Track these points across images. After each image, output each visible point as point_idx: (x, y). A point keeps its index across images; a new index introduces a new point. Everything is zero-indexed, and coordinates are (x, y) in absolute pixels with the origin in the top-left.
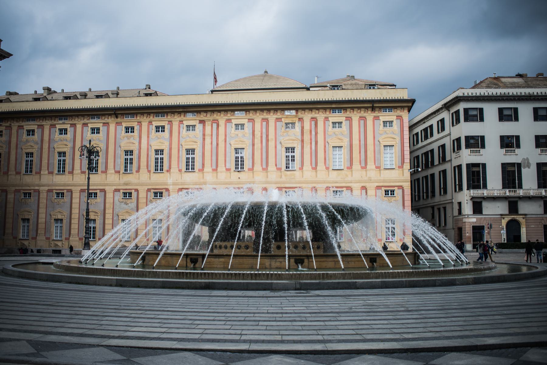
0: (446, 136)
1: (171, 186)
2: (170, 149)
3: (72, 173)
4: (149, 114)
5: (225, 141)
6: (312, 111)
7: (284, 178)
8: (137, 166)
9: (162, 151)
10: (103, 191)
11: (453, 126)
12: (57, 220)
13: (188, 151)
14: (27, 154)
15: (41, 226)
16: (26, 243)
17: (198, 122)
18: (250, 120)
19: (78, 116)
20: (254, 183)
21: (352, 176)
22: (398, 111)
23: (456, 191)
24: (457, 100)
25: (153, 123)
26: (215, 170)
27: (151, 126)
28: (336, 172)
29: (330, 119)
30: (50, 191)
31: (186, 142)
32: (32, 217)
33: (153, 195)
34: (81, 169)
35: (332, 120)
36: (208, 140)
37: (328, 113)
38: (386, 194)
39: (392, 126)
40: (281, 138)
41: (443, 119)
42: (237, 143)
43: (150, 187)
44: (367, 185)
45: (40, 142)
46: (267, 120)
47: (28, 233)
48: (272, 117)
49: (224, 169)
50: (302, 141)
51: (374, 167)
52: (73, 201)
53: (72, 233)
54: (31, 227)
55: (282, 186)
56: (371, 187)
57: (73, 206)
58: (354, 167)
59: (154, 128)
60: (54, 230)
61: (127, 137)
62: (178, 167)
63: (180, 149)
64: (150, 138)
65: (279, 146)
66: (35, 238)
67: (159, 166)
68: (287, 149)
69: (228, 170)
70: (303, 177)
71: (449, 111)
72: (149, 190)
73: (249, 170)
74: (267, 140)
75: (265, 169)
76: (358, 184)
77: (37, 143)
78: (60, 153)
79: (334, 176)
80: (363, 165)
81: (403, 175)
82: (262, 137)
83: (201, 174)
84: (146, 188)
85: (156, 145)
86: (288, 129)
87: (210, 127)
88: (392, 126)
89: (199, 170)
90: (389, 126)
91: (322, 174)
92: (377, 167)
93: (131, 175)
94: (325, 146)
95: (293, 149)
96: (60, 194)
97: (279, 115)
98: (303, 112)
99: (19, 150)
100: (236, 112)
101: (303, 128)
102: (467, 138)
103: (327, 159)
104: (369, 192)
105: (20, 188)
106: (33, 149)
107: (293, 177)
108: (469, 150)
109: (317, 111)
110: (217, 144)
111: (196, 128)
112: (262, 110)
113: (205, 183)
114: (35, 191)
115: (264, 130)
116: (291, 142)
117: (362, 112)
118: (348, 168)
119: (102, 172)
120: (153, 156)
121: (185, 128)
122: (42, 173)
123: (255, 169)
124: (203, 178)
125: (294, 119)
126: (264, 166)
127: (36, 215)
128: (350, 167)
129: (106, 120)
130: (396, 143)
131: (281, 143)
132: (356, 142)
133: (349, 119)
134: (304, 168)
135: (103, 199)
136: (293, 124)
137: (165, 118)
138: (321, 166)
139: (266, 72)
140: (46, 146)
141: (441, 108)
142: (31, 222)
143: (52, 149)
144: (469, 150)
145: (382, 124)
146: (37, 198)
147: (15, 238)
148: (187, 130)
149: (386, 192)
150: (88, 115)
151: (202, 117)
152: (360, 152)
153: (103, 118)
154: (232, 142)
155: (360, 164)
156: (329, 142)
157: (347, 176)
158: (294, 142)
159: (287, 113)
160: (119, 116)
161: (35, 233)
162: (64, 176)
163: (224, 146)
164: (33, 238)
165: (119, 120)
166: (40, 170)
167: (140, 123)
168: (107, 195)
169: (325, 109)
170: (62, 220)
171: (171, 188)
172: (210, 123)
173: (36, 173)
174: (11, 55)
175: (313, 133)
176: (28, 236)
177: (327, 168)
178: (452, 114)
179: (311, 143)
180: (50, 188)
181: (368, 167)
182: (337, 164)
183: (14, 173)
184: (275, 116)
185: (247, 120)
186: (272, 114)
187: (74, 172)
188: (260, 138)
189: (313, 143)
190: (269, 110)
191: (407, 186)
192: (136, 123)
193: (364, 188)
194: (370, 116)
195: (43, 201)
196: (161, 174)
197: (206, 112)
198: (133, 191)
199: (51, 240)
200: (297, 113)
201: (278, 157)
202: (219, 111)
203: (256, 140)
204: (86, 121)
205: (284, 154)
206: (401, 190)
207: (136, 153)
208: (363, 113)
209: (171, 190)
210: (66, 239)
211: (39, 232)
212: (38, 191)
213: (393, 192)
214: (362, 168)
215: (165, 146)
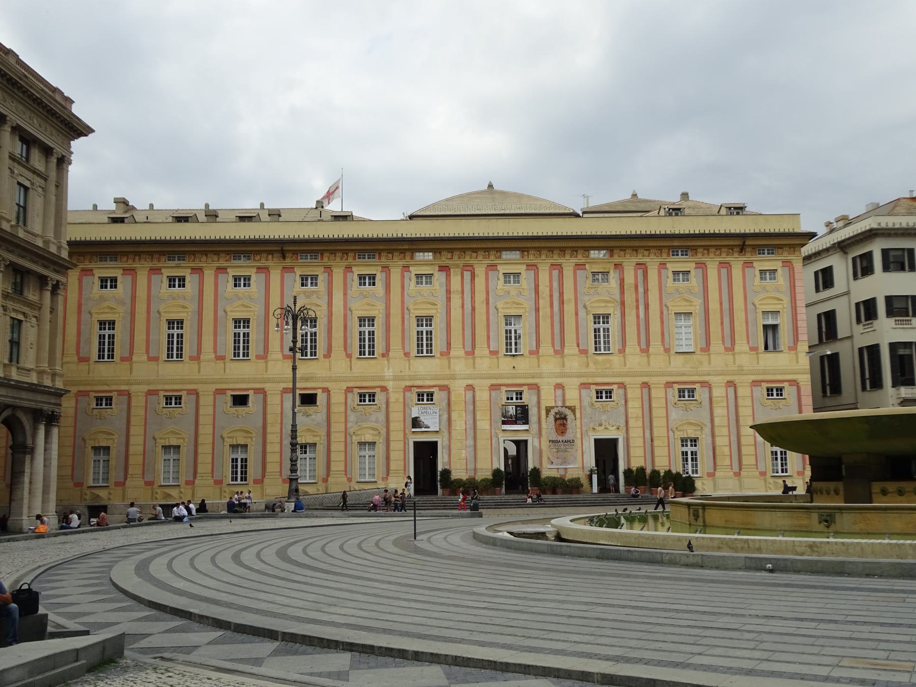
0: (837, 297)
1: (391, 383)
2: (388, 316)
3: (196, 358)
4: (346, 252)
5: (488, 303)
6: (636, 251)
7: (592, 368)
8: (326, 346)
9: (372, 320)
10: (262, 392)
11: (855, 277)
12: (166, 448)
13: (420, 320)
14: (102, 323)
15: (135, 461)
16: (103, 493)
17: (437, 268)
18: (531, 266)
19: (206, 253)
20: (540, 376)
21: (710, 363)
22: (785, 254)
23: (864, 388)
24: (871, 235)
25: (354, 269)
26: (471, 353)
27: (349, 275)
28: (682, 357)
29: (668, 265)
30: (151, 393)
31: (415, 304)
32: (115, 444)
33: (357, 398)
34: (215, 351)
35: (672, 267)
36: (456, 301)
37: (664, 255)
38: (768, 395)
39: (775, 279)
40: (586, 298)
41: (831, 268)
42: (509, 306)
43: (351, 384)
44: (736, 379)
45: (128, 301)
46: (559, 267)
47: (107, 473)
48: (568, 263)
49: (488, 352)
50: (623, 303)
51: (747, 348)
52: (201, 412)
53: (199, 471)
54: (113, 463)
55: (590, 380)
56: (744, 382)
57: (202, 420)
58: (712, 348)
59: (356, 278)
60: (161, 466)
61: (305, 293)
62: (403, 348)
63: (406, 317)
64: (349, 296)
65: (582, 313)
66: (121, 484)
67: (367, 348)
68: (596, 317)
69: (494, 353)
70: (625, 365)
71: (846, 253)
72: (349, 390)
73: (531, 353)
74: (562, 302)
75: (560, 352)
76: (721, 377)
77: (122, 303)
78: (171, 323)
79: (678, 363)
81: (797, 362)
82: (551, 296)
83: (445, 361)
84: (344, 385)
85: (359, 309)
86: (596, 283)
87: (459, 278)
88: (775, 279)
89: (442, 354)
91: (658, 360)
92: (752, 349)
93: (314, 362)
94: (662, 313)
95: (606, 318)
96: (174, 400)
97: (580, 259)
98: (622, 253)
99: (85, 316)
100: (504, 253)
101: (622, 281)
102: (889, 300)
103: (666, 334)
104: (741, 392)
105: (89, 388)
106: (114, 313)
107: (608, 365)
108: (894, 319)
109: (646, 253)
110: (473, 309)
111: (434, 279)
112: (551, 250)
113: (453, 377)
114: (121, 393)
115: (555, 285)
116: (603, 305)
117: (724, 255)
118: (702, 350)
119: (258, 357)
120: (355, 328)
121: (414, 279)
122: (134, 358)
123: (540, 351)
124: (449, 367)
125: (608, 266)
126: (558, 347)
127: (123, 439)
128: (706, 349)
129: (263, 263)
130: (784, 308)
131: (585, 307)
132: (714, 306)
133: (701, 265)
134: (627, 350)
135: (261, 406)
136: (606, 273)
137: (376, 261)
138: (656, 346)
139: (490, 186)
140: (141, 308)
141: (827, 250)
142: (113, 452)
143: (153, 315)
144: (891, 321)
145: (758, 273)
146: (125, 407)
147: (79, 485)
148: (418, 283)
149: (768, 390)
150: (228, 253)
151: (445, 260)
152: (722, 323)
153: (258, 257)
154: (500, 305)
155: (724, 344)
156: (668, 304)
157: (701, 363)
158: (609, 305)
159: (594, 254)
160: (290, 255)
161: (122, 474)
162: (180, 365)
163: (484, 310)
164: (117, 484)
165: (288, 262)
166: (131, 353)
167: (328, 269)
168: (269, 399)
169: (660, 249)
170: (179, 447)
171: (390, 385)
172: (459, 271)
173: (123, 359)
174: (92, 131)
175: (641, 290)
176: (106, 479)
177: (667, 350)
178: (854, 259)
179: (637, 307)
180: (152, 387)
181: (737, 348)
182: (684, 342)
183: (75, 359)
184: (574, 261)
185: (524, 267)
186: (567, 257)
187: (202, 357)
188: (548, 299)
189: (642, 308)
190: (563, 250)
191: (805, 380)
192: (322, 269)
193: (731, 384)
194: (737, 263)
195: (138, 411)
196: (371, 361)
197: (451, 251)
198: (319, 392)
199: (156, 486)
200: (611, 256)
201: (580, 331)
202: (475, 250)
203: (541, 302)
204: (222, 263)
205: (592, 326)
206: (795, 388)
207: (322, 323)
208: (725, 258)
209: (391, 390)
210: (187, 483)
211: (130, 471)
212: (128, 394)
213: (780, 390)
214: (727, 349)
215: (378, 311)
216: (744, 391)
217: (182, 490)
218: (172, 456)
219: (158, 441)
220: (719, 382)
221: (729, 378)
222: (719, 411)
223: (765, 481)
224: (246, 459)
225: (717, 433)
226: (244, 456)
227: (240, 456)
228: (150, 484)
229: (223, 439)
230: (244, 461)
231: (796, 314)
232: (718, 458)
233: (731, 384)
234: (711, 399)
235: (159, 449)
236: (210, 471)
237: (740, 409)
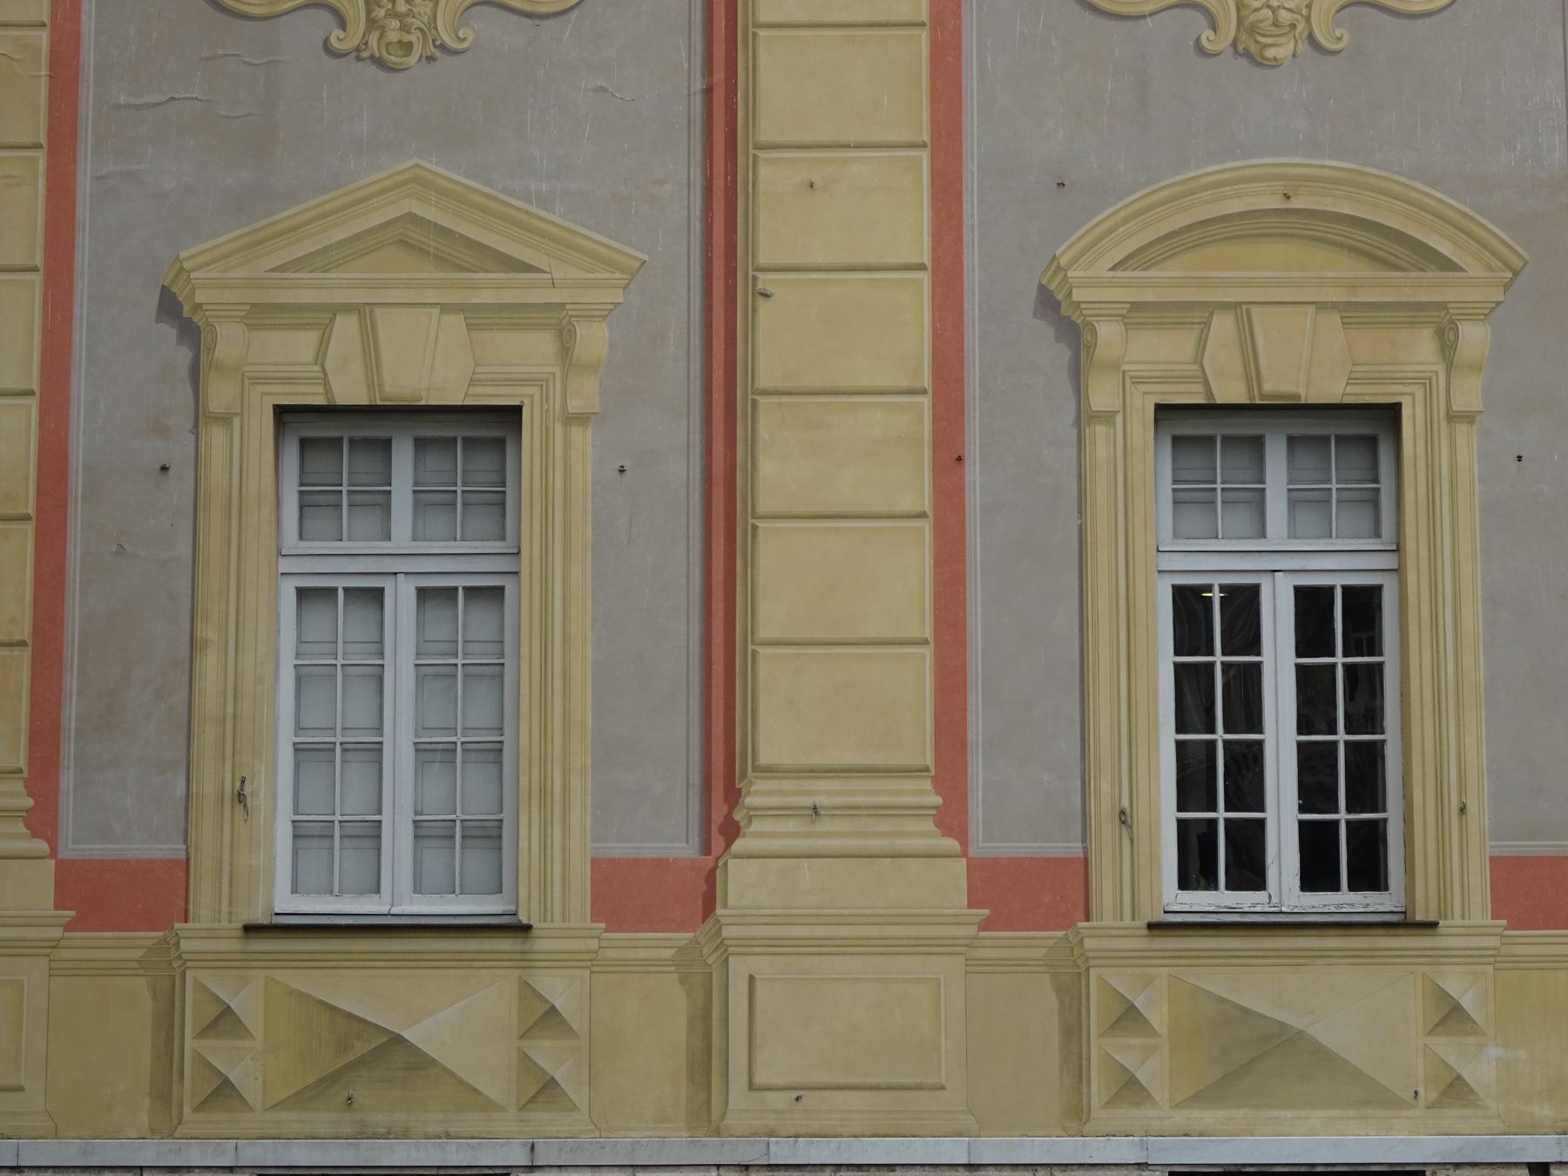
53: (776, 736)
60: (267, 657)
199: (210, 921)
210: (663, 897)
217: (560, 989)
218: (406, 541)
219: (228, 341)
224: (1364, 603)
226: (1339, 563)
227: (1284, 551)
228: (124, 897)
229: (1073, 332)
230: (1344, 621)
235: (248, 457)
236: (919, 746)
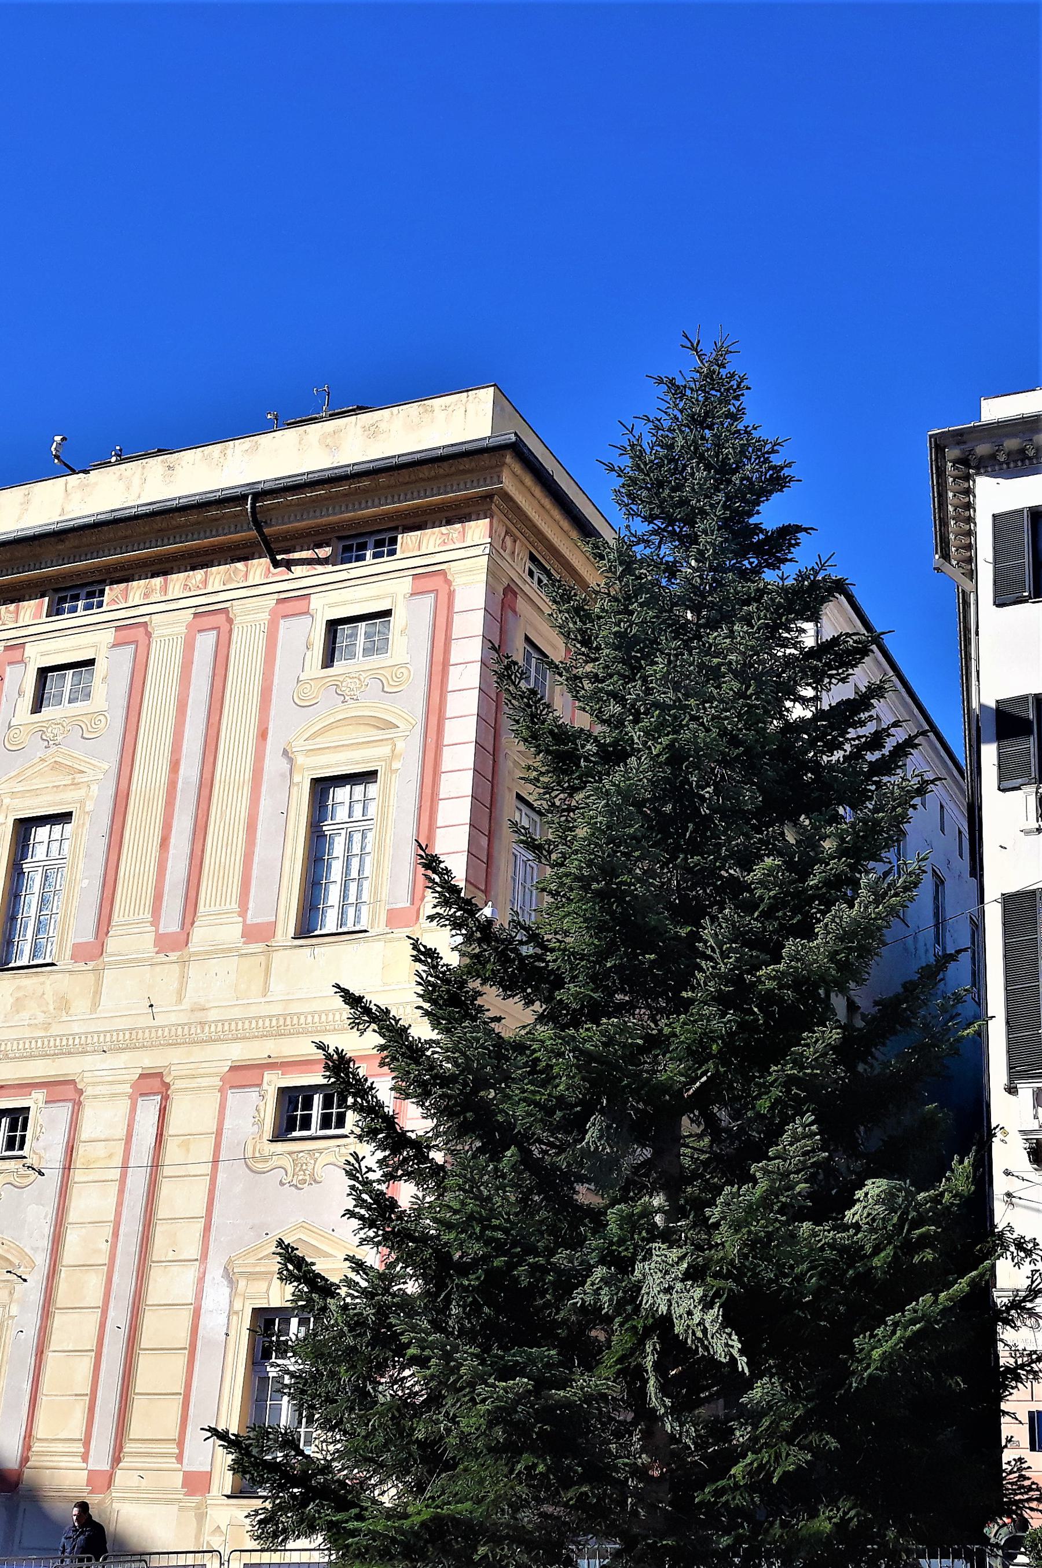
21: (95, 1005)
29: (30, 650)
51: (232, 932)
76: (122, 1059)
80: (170, 923)
90: (367, 652)
155: (155, 921)
157: (64, 1004)
181: (200, 935)
214: (166, 944)
216: (191, 1113)
220: (106, 1075)
221: (149, 1061)
222: (92, 1201)
223: (201, 1517)
225: (63, 1295)
231: (436, 773)
232: (44, 1402)
233: (155, 1085)
234: (70, 1150)
237: (166, 1190)
